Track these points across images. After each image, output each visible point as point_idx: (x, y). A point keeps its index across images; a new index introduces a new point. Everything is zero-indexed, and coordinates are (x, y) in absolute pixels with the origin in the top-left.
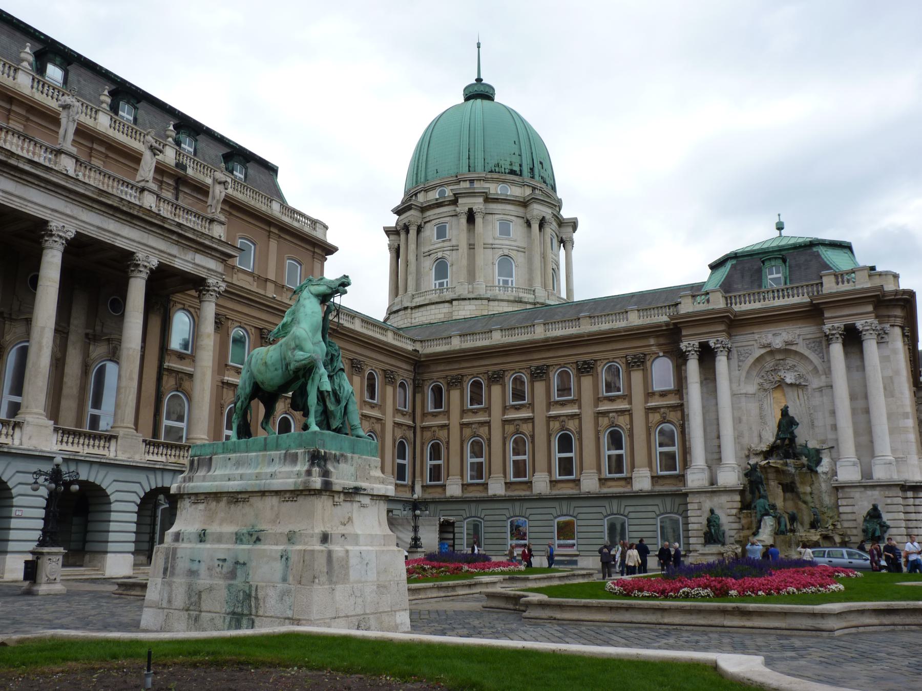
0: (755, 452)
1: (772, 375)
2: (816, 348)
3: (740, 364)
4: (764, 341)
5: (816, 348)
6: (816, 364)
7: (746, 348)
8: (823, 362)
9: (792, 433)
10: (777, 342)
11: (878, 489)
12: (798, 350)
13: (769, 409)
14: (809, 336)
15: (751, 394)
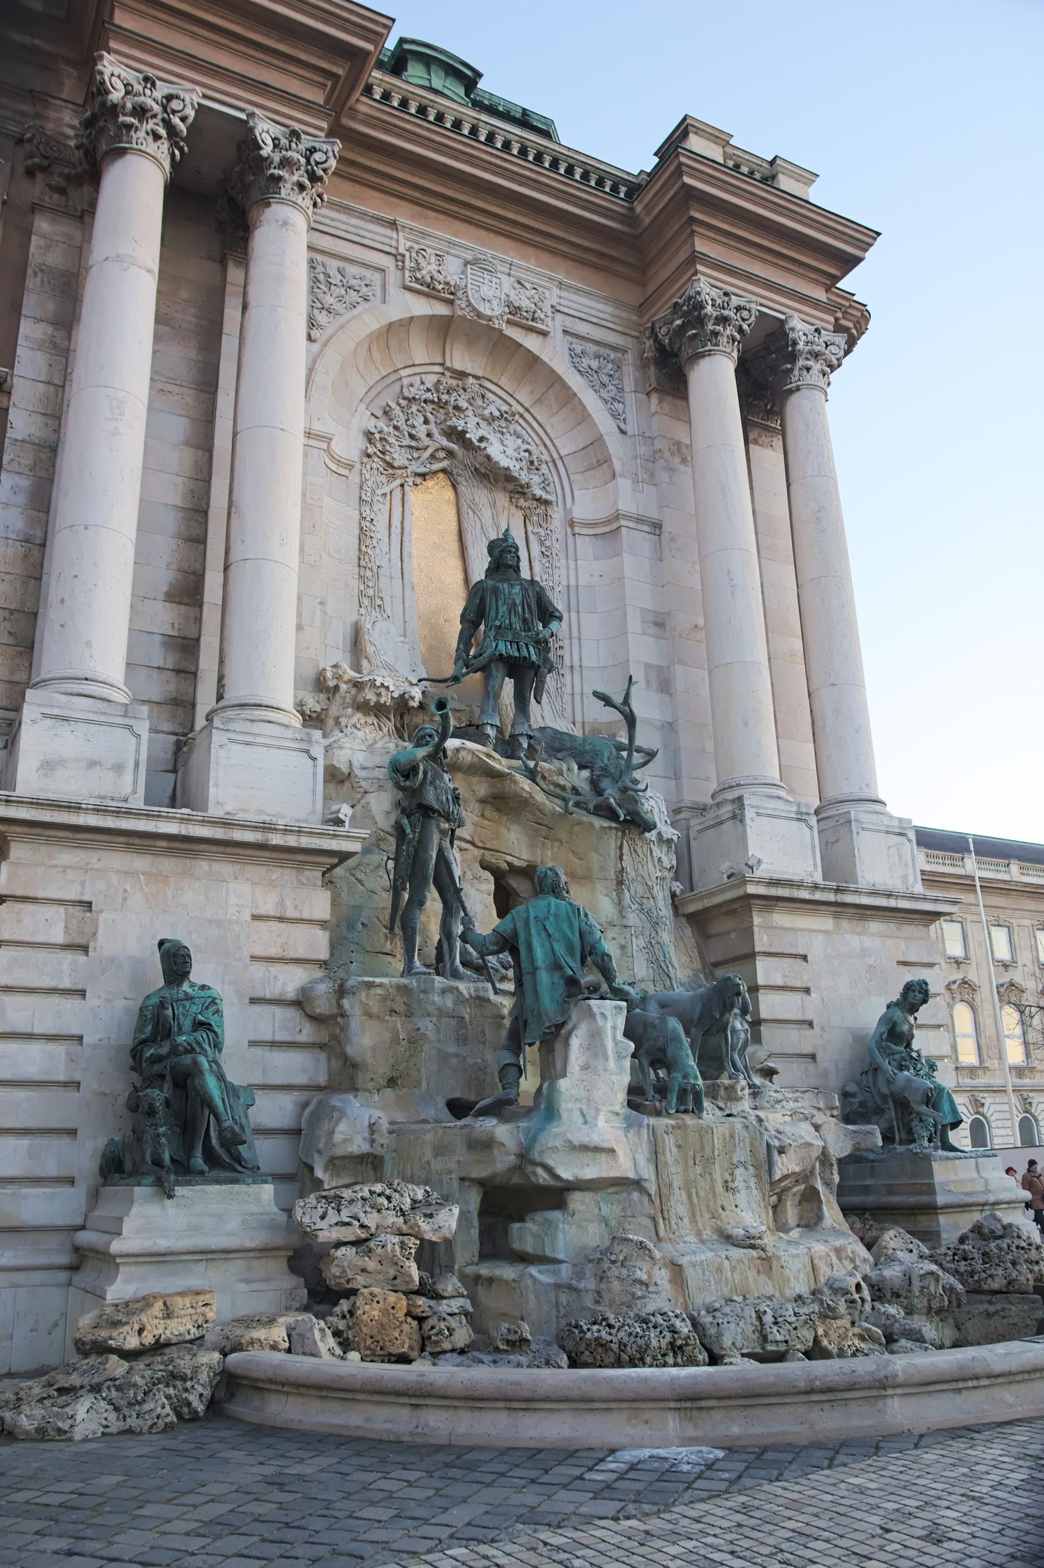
0: (370, 696)
1: (426, 422)
2: (605, 379)
3: (322, 318)
4: (429, 268)
5: (605, 379)
6: (602, 429)
7: (352, 270)
8: (623, 432)
9: (542, 645)
10: (486, 291)
11: (875, 926)
12: (544, 357)
13: (396, 552)
14: (583, 329)
15: (339, 463)
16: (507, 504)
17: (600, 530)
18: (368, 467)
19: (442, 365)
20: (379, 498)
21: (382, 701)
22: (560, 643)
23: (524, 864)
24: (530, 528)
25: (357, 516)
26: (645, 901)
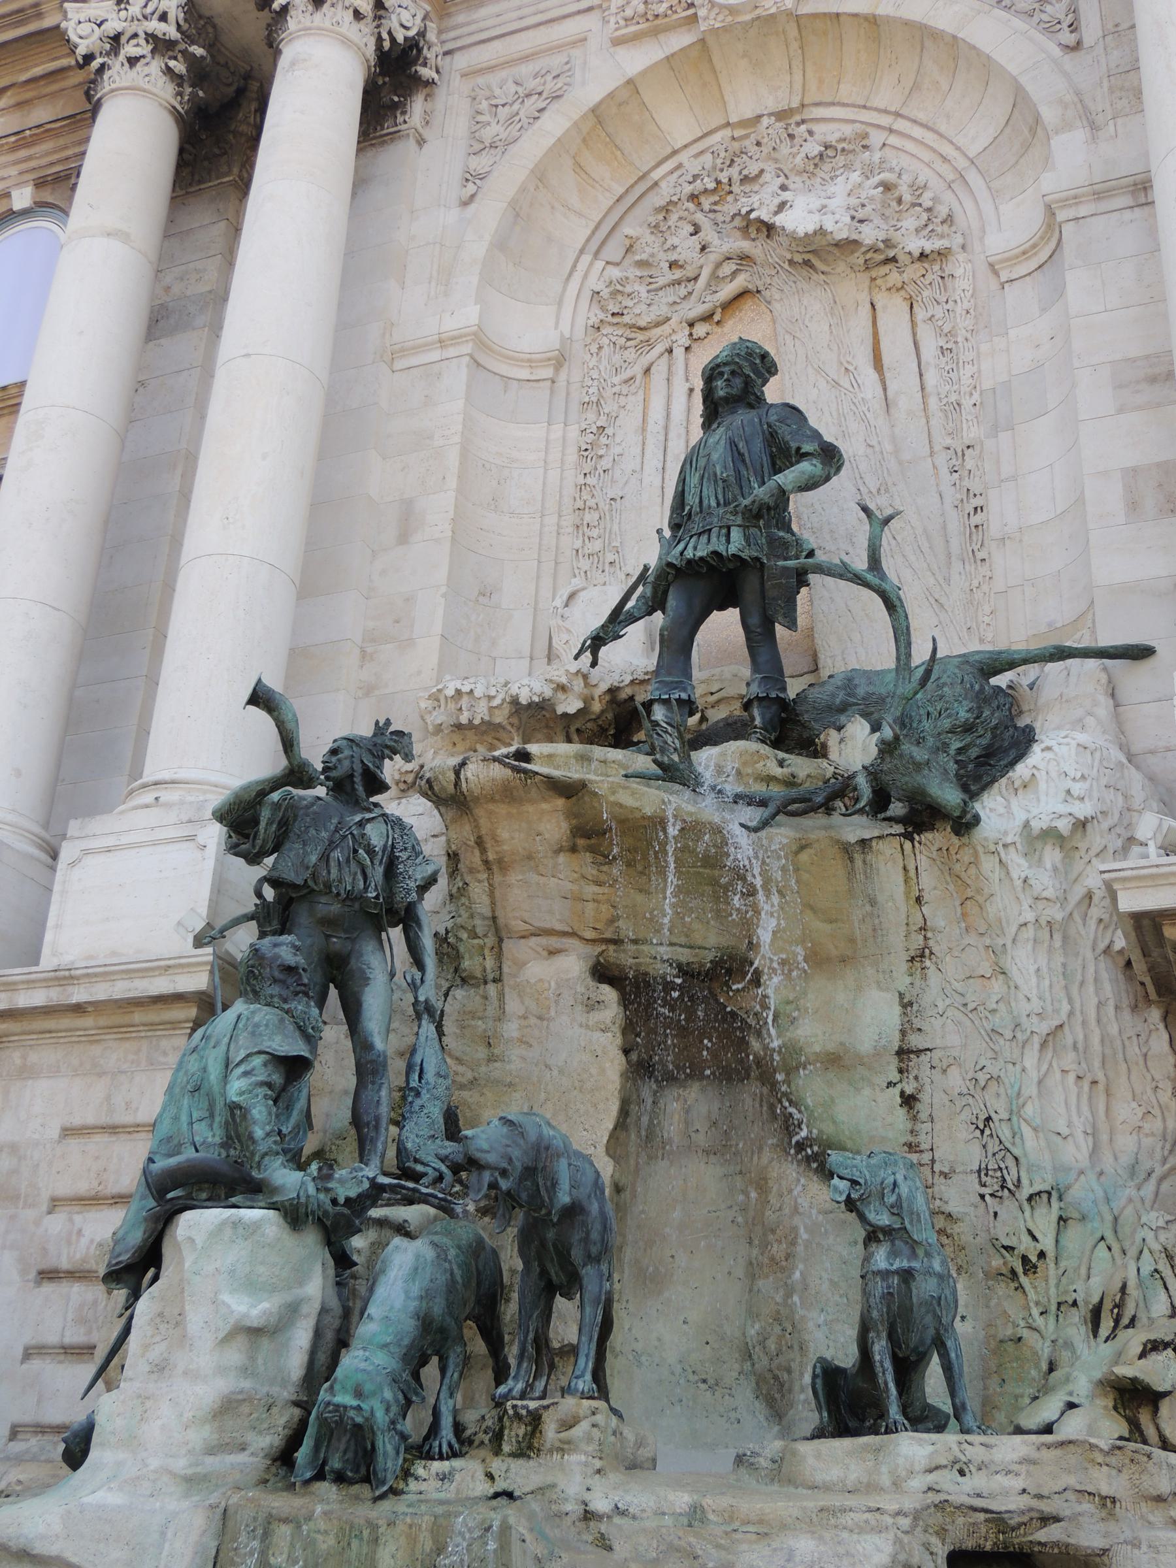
1: (696, 231)
3: (480, 163)
6: (1012, 68)
7: (526, 70)
15: (531, 363)
16: (864, 298)
17: (1043, 256)
18: (594, 349)
19: (728, 124)
20: (616, 389)
21: (464, 719)
22: (977, 502)
23: (710, 956)
24: (920, 314)
25: (573, 432)
26: (976, 984)
